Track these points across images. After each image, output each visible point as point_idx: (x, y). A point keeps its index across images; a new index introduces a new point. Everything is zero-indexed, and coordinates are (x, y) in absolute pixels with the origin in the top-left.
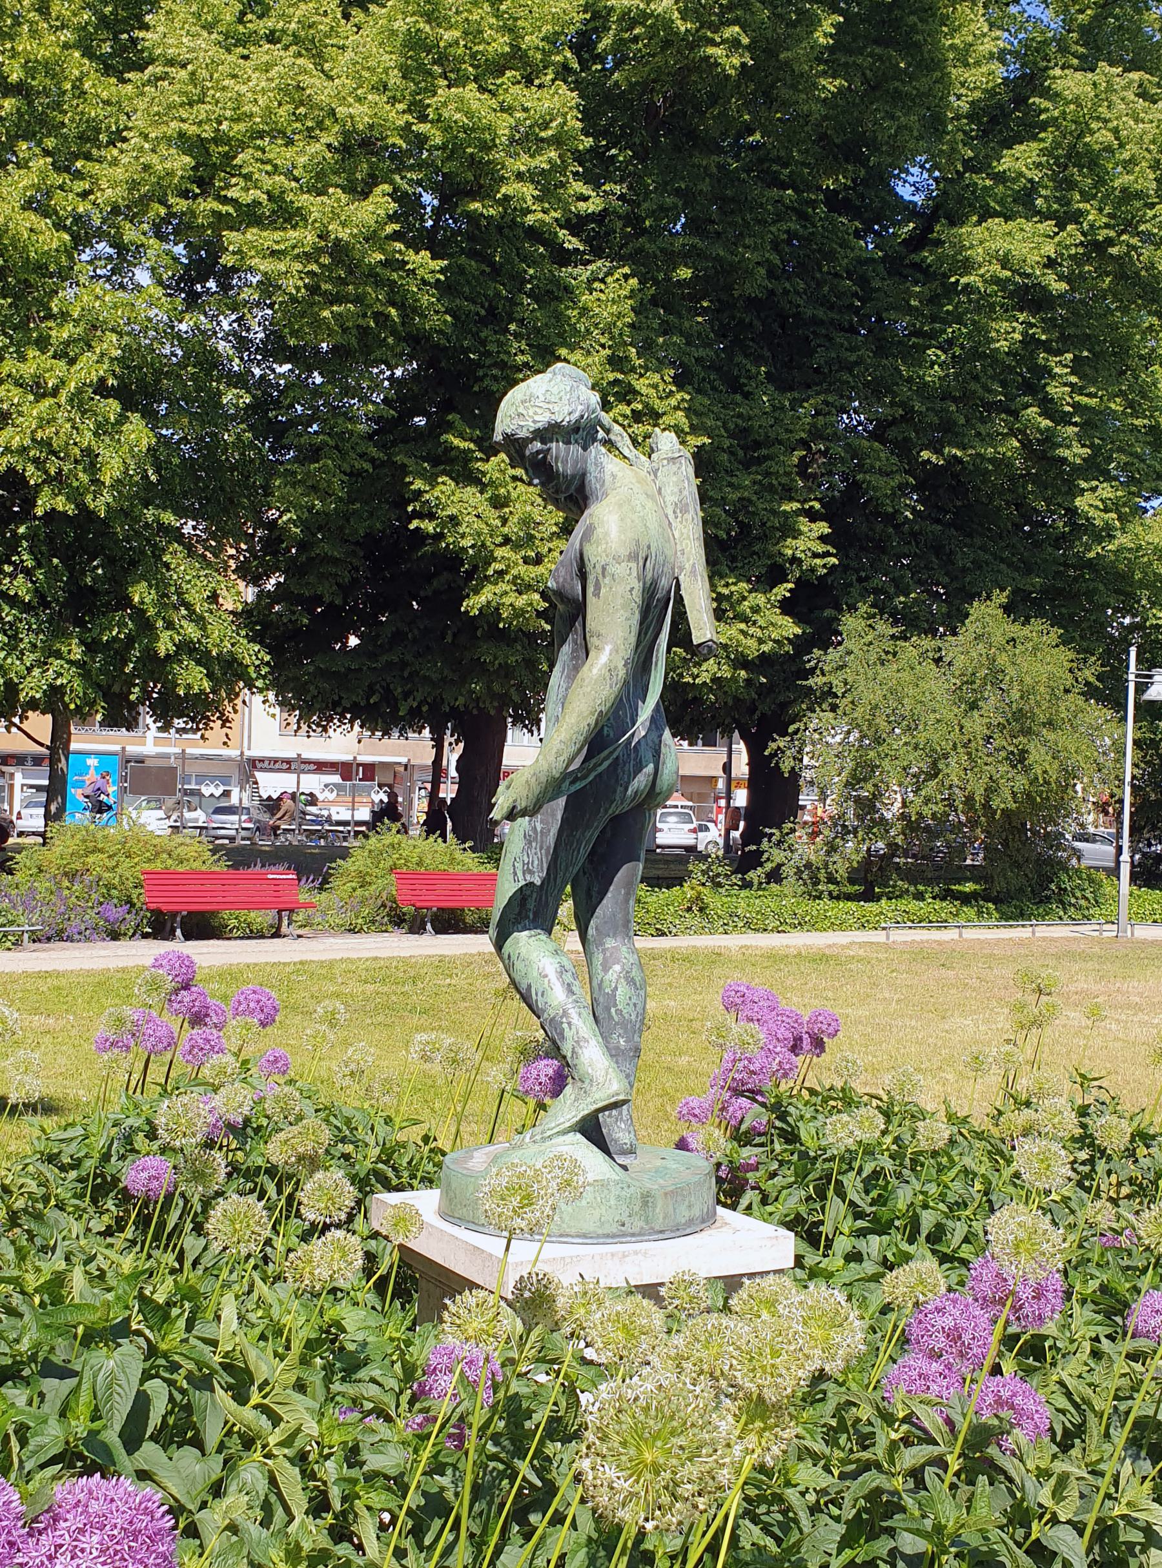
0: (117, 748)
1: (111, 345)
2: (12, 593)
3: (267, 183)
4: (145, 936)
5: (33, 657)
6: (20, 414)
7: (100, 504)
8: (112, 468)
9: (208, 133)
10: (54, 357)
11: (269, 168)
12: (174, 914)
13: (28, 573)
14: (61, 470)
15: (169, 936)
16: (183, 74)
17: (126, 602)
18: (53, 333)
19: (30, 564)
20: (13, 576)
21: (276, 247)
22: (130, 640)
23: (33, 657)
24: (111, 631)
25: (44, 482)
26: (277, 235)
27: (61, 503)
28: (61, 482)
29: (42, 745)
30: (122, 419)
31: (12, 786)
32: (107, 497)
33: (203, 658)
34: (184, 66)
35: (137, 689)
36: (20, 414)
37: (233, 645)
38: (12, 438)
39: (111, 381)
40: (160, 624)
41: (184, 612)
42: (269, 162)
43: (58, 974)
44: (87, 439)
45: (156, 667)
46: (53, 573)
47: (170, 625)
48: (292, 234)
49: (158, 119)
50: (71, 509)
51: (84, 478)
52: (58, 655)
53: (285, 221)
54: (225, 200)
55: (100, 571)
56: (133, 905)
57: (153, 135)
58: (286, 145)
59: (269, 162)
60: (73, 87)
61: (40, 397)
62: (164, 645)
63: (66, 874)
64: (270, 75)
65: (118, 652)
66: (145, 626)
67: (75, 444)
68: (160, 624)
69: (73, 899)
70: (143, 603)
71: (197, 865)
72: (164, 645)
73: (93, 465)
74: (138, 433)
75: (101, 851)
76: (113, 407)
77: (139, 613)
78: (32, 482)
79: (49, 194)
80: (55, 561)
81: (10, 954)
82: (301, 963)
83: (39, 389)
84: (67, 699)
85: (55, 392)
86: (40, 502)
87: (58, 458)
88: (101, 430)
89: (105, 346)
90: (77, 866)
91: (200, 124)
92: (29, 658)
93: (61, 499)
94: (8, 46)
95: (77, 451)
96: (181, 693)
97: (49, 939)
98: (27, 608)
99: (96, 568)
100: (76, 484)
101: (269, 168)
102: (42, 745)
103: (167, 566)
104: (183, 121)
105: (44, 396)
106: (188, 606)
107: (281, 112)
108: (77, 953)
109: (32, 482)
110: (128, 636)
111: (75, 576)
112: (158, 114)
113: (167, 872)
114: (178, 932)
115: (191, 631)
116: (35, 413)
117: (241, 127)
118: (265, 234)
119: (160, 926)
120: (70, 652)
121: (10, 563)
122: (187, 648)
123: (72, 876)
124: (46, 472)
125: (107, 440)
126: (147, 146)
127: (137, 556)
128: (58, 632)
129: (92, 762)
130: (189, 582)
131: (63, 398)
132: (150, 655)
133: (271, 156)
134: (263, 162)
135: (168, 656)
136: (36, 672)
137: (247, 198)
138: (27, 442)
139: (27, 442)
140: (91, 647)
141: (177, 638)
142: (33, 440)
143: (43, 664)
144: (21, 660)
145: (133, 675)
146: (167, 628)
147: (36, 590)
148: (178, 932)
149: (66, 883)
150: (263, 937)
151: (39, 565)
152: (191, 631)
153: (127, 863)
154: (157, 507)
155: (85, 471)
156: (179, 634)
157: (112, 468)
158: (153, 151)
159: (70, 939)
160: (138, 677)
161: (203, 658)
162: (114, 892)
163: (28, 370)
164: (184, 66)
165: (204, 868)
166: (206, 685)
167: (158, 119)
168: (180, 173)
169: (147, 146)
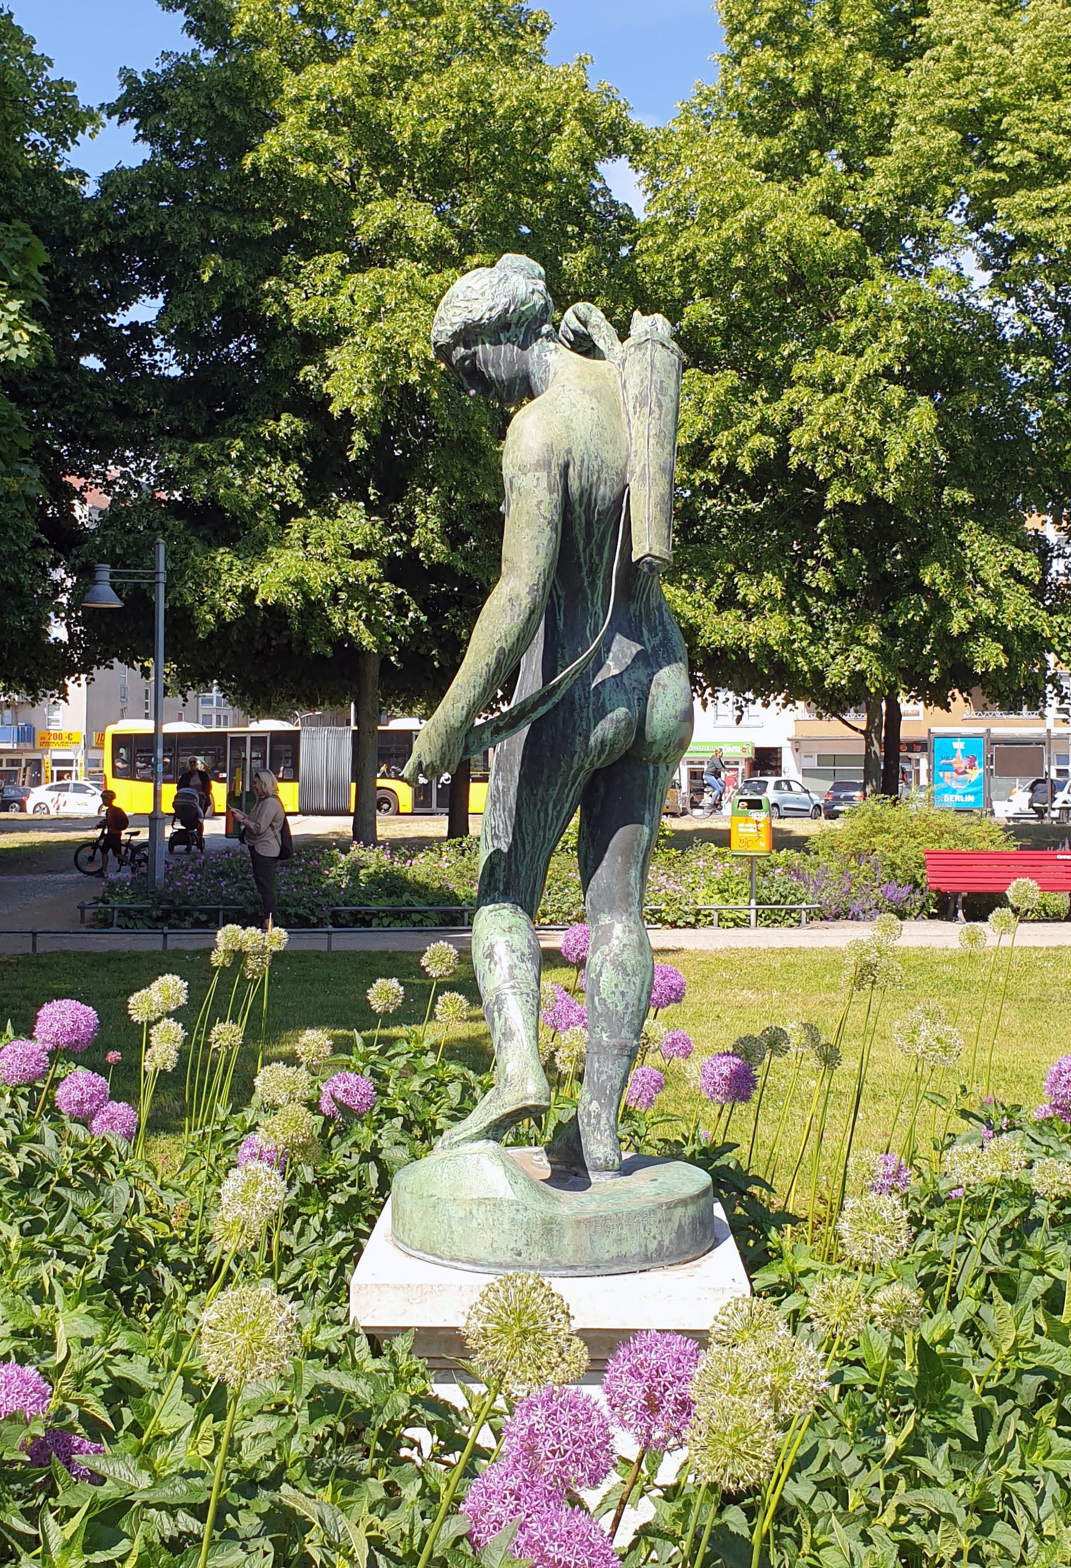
0: (982, 730)
1: (896, 333)
2: (814, 585)
3: (1034, 142)
4: (932, 916)
5: (836, 645)
6: (810, 413)
7: (889, 491)
8: (897, 452)
9: (974, 103)
10: (844, 353)
11: (1037, 126)
12: (956, 894)
13: (827, 564)
14: (848, 462)
15: (952, 917)
16: (950, 51)
17: (918, 586)
18: (842, 330)
19: (830, 556)
20: (814, 569)
21: (1046, 205)
22: (927, 621)
23: (836, 645)
24: (907, 614)
25: (835, 475)
26: (1046, 193)
27: (848, 495)
28: (849, 475)
29: (856, 729)
30: (908, 404)
31: (918, 771)
32: (895, 483)
33: (999, 634)
34: (949, 42)
35: (936, 670)
36: (810, 413)
37: (1031, 618)
38: (802, 436)
39: (897, 368)
40: (954, 603)
41: (979, 589)
42: (1035, 119)
43: (801, 950)
44: (873, 428)
45: (954, 649)
46: (852, 563)
47: (964, 604)
48: (1061, 188)
49: (925, 100)
50: (859, 499)
51: (871, 466)
52: (857, 641)
53: (1057, 176)
54: (995, 168)
55: (899, 557)
56: (917, 885)
57: (920, 117)
58: (1054, 100)
59: (1035, 119)
60: (858, 88)
61: (828, 393)
62: (958, 623)
63: (853, 855)
64: (1036, 32)
65: (916, 633)
66: (941, 608)
67: (861, 435)
68: (954, 603)
69: (861, 879)
70: (935, 584)
71: (985, 845)
72: (958, 623)
73: (880, 452)
74: (923, 415)
75: (888, 831)
76: (896, 393)
77: (929, 592)
78: (821, 477)
79: (838, 197)
80: (855, 551)
81: (790, 930)
82: (1057, 949)
83: (827, 386)
84: (868, 683)
85: (843, 387)
86: (829, 496)
87: (846, 450)
88: (887, 416)
89: (890, 334)
90: (864, 846)
91: (966, 96)
92: (834, 646)
93: (849, 491)
94: (797, 62)
95: (862, 441)
96: (979, 671)
97: (837, 917)
98: (831, 599)
99: (896, 553)
100: (864, 474)
101: (1037, 126)
102: (856, 729)
103: (961, 544)
104: (950, 97)
105: (834, 390)
106: (983, 582)
107: (1047, 66)
108: (842, 931)
109: (821, 477)
110: (924, 618)
111: (875, 564)
112: (924, 96)
113: (949, 852)
114: (960, 913)
115: (986, 606)
116: (821, 411)
117: (1007, 90)
118: (1034, 194)
119: (944, 908)
120: (867, 636)
121: (813, 557)
122: (981, 625)
123: (858, 855)
124: (835, 466)
125: (893, 426)
126: (913, 129)
127: (933, 538)
128: (861, 618)
129: (959, 745)
130: (983, 558)
131: (849, 392)
132: (944, 634)
133: (1037, 113)
134: (1029, 121)
135: (961, 634)
136: (839, 659)
137: (1013, 161)
138: (816, 439)
139: (816, 439)
140: (890, 632)
141: (971, 616)
142: (821, 436)
143: (844, 651)
144: (826, 648)
145: (931, 657)
146: (962, 607)
147: (837, 581)
148: (960, 913)
149: (853, 863)
150: (1060, 920)
151: (839, 557)
152: (986, 606)
153: (913, 842)
154: (954, 486)
155: (872, 460)
156: (973, 611)
157: (897, 452)
158: (922, 133)
159: (855, 918)
160: (936, 657)
161: (999, 634)
162: (898, 872)
163: (816, 370)
164: (949, 42)
165: (993, 849)
166: (1003, 661)
167: (925, 100)
168: (946, 150)
169: (913, 129)
